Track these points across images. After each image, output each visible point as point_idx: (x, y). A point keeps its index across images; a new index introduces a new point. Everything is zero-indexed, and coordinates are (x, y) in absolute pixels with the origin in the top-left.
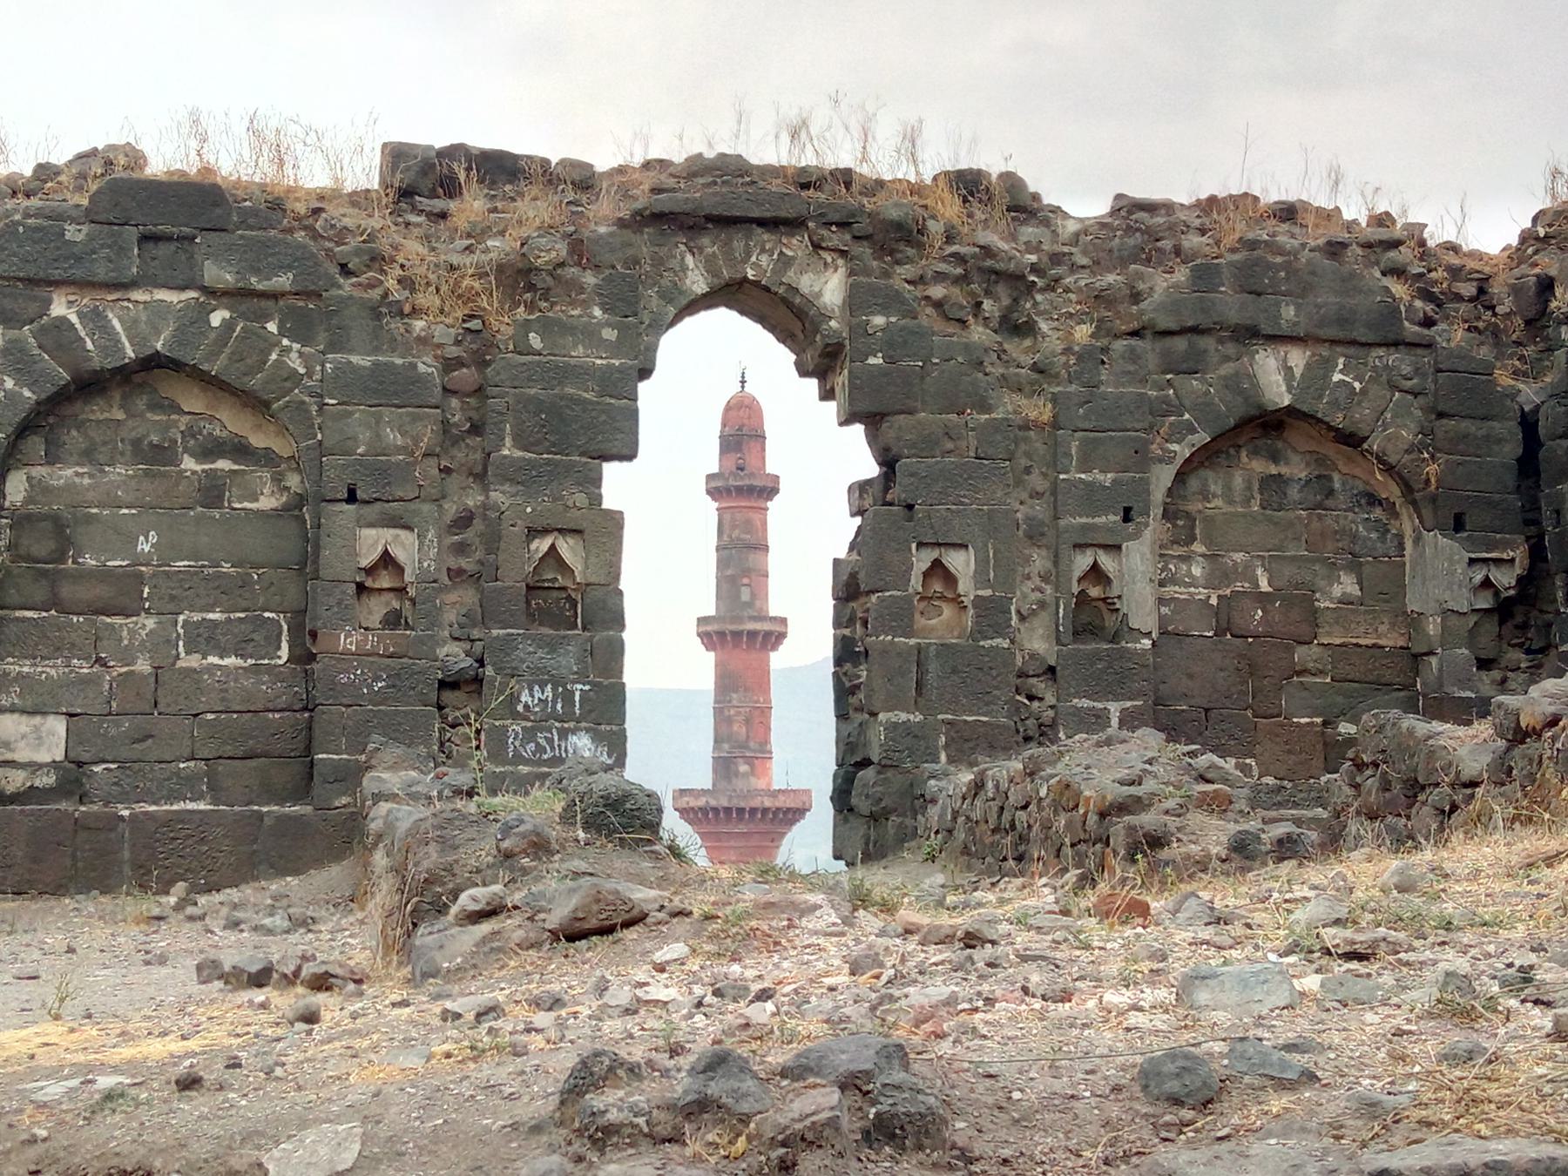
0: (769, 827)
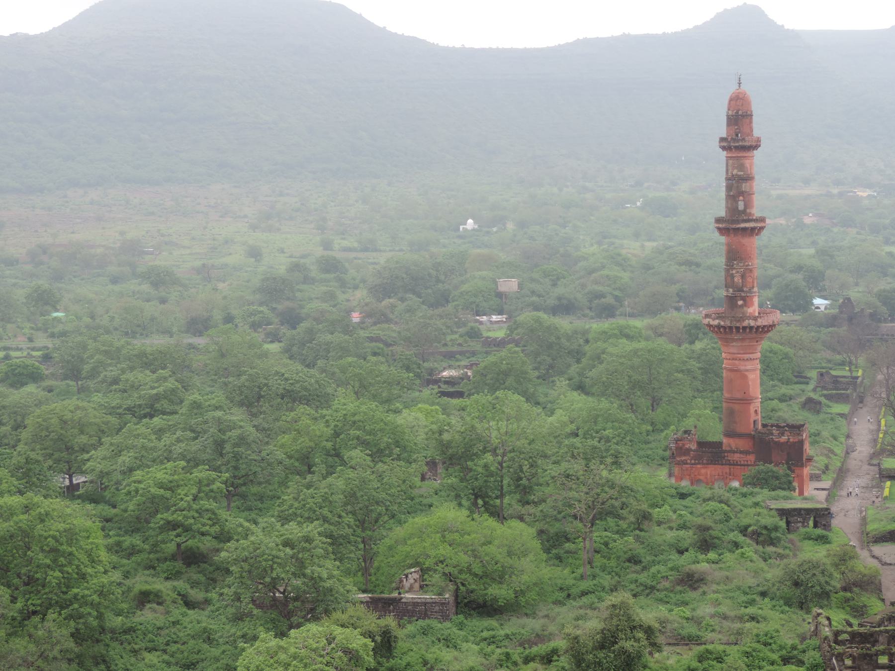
0: (754, 335)
